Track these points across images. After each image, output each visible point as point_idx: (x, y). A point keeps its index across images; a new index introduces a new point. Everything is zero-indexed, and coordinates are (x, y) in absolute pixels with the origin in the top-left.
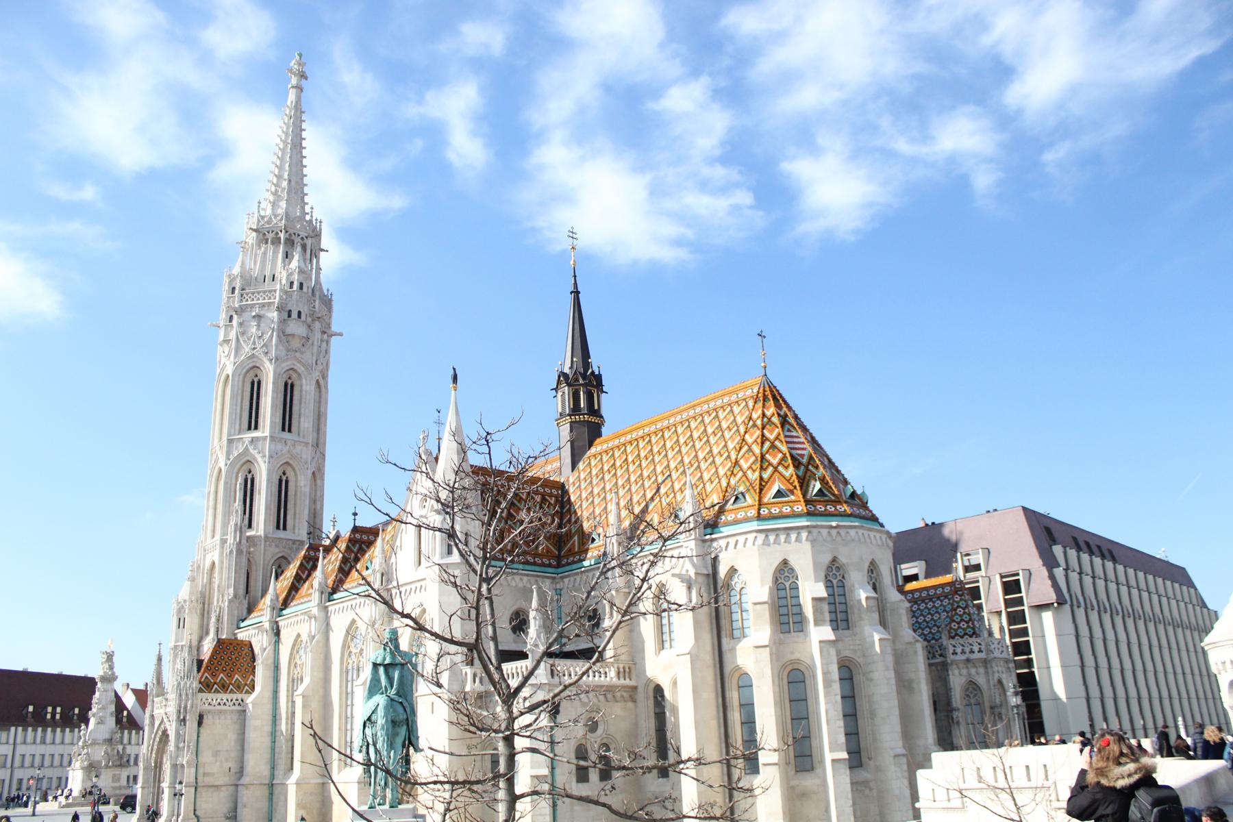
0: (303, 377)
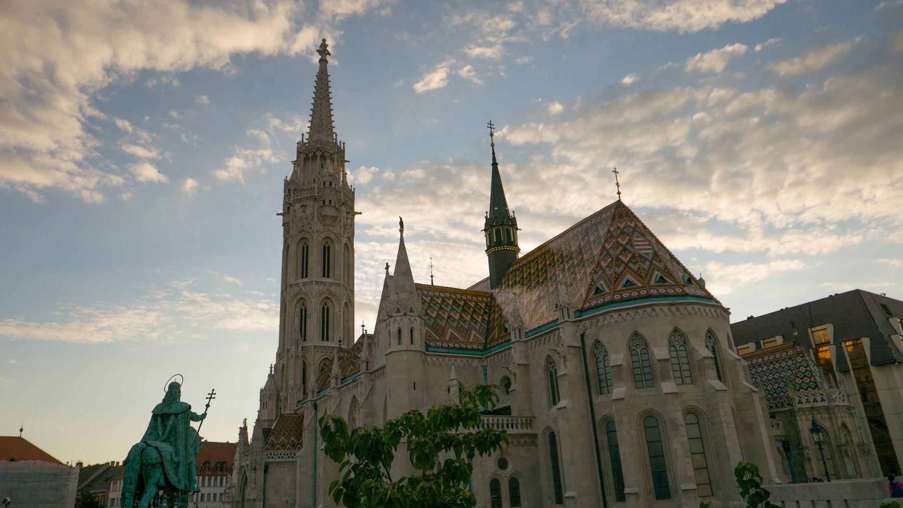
0: (335, 241)
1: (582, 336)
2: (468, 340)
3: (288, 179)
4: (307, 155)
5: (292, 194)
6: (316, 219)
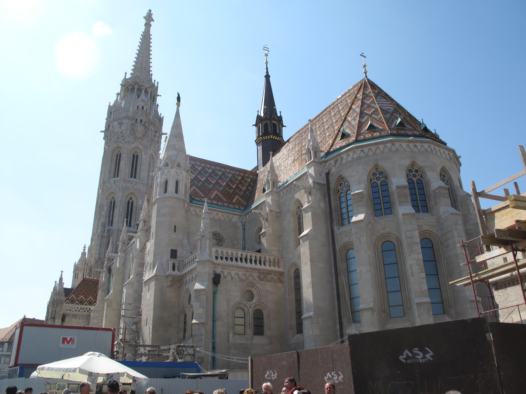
1: (328, 174)
2: (231, 201)
3: (111, 104)
4: (128, 87)
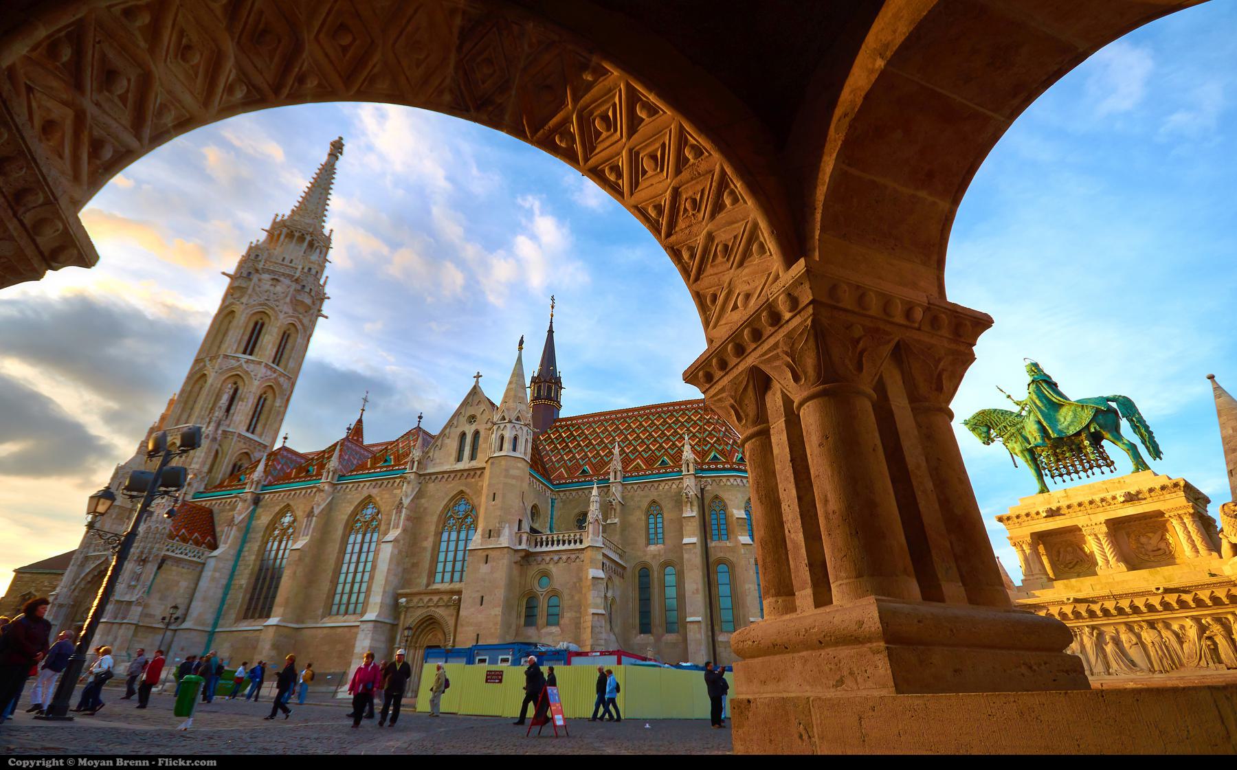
5: (263, 261)
6: (288, 300)
